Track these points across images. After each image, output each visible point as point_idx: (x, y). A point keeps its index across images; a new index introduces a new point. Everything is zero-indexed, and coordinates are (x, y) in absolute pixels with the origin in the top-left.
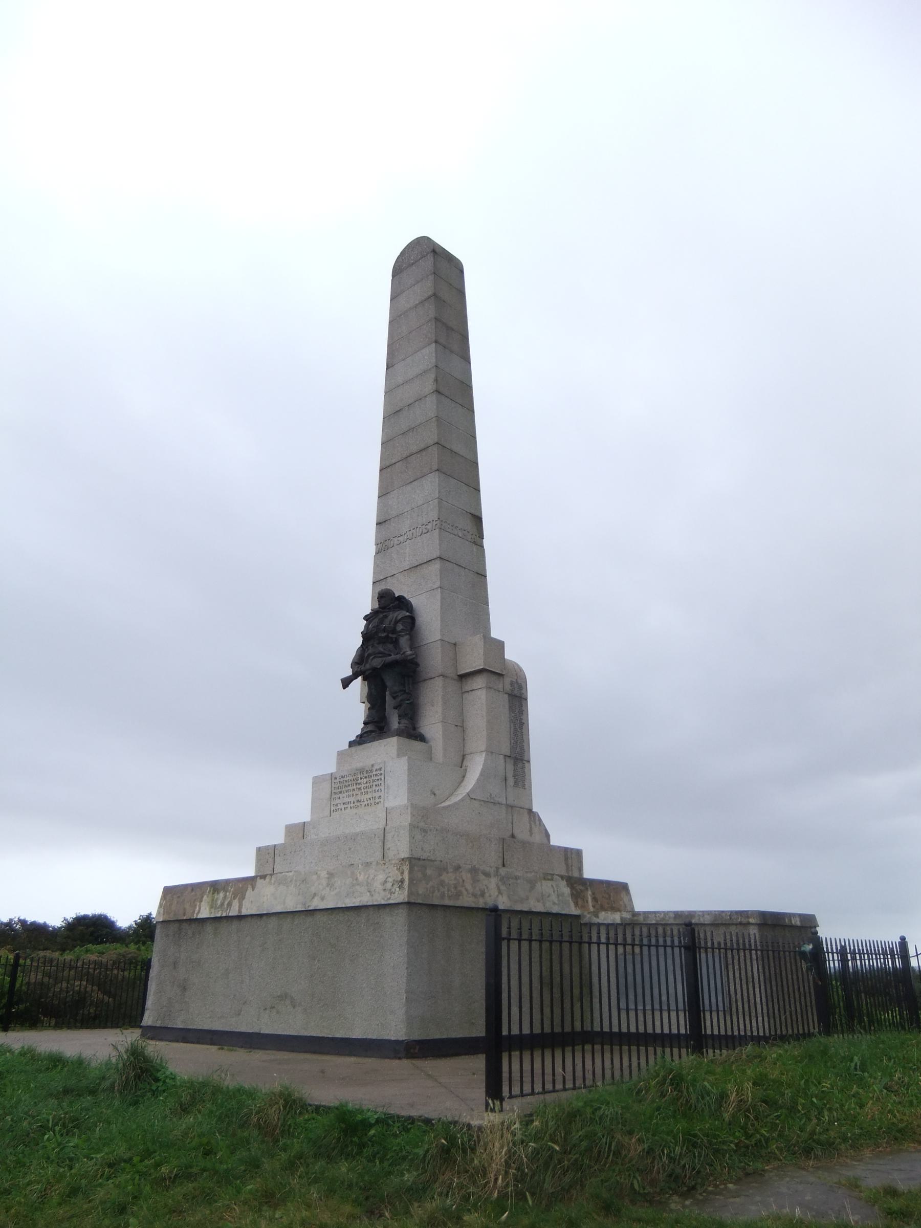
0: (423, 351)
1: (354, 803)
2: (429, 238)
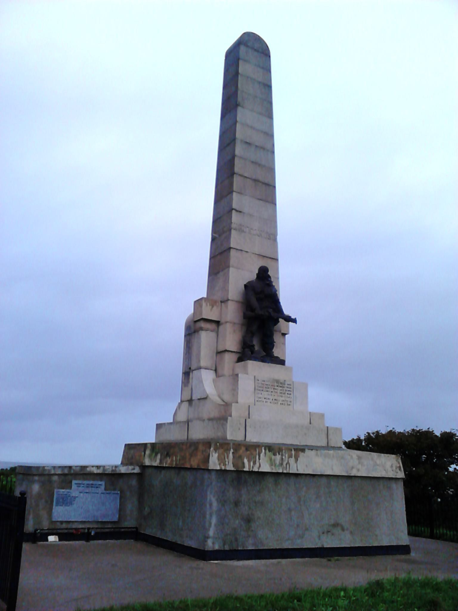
1: (272, 400)
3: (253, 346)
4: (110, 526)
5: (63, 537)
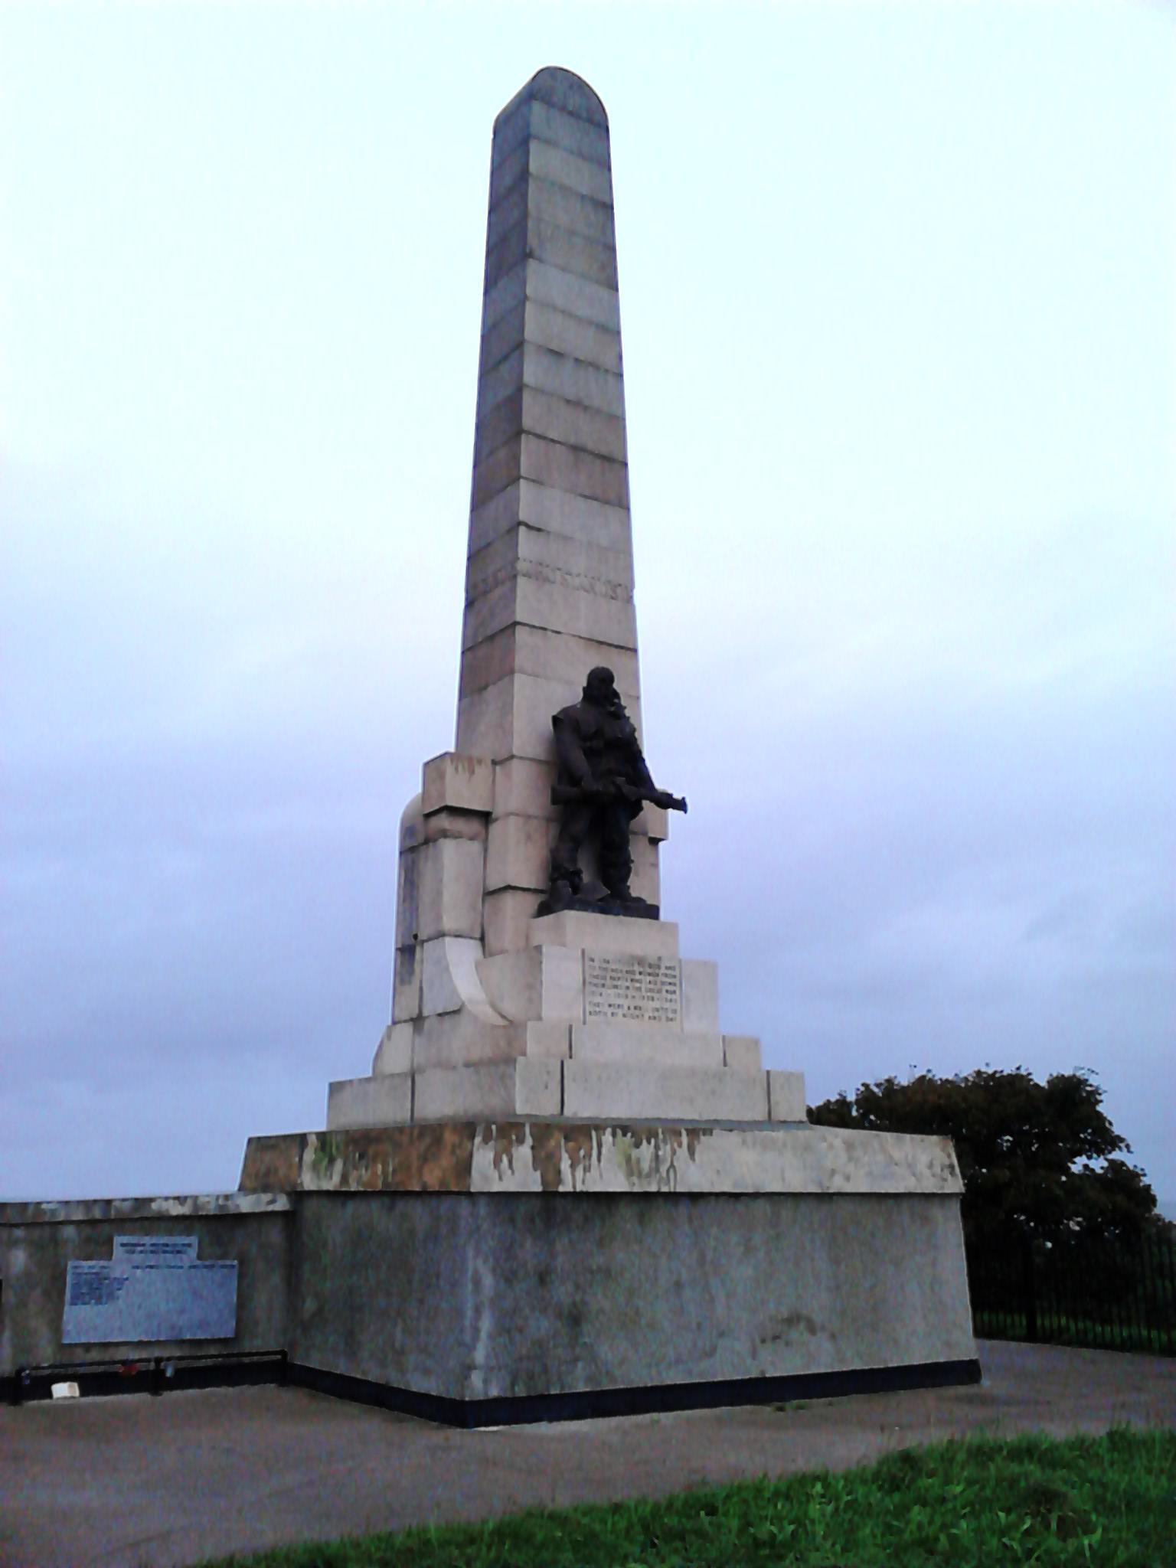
1: (629, 1008)
3: (578, 873)
4: (213, 1351)
5: (91, 1384)
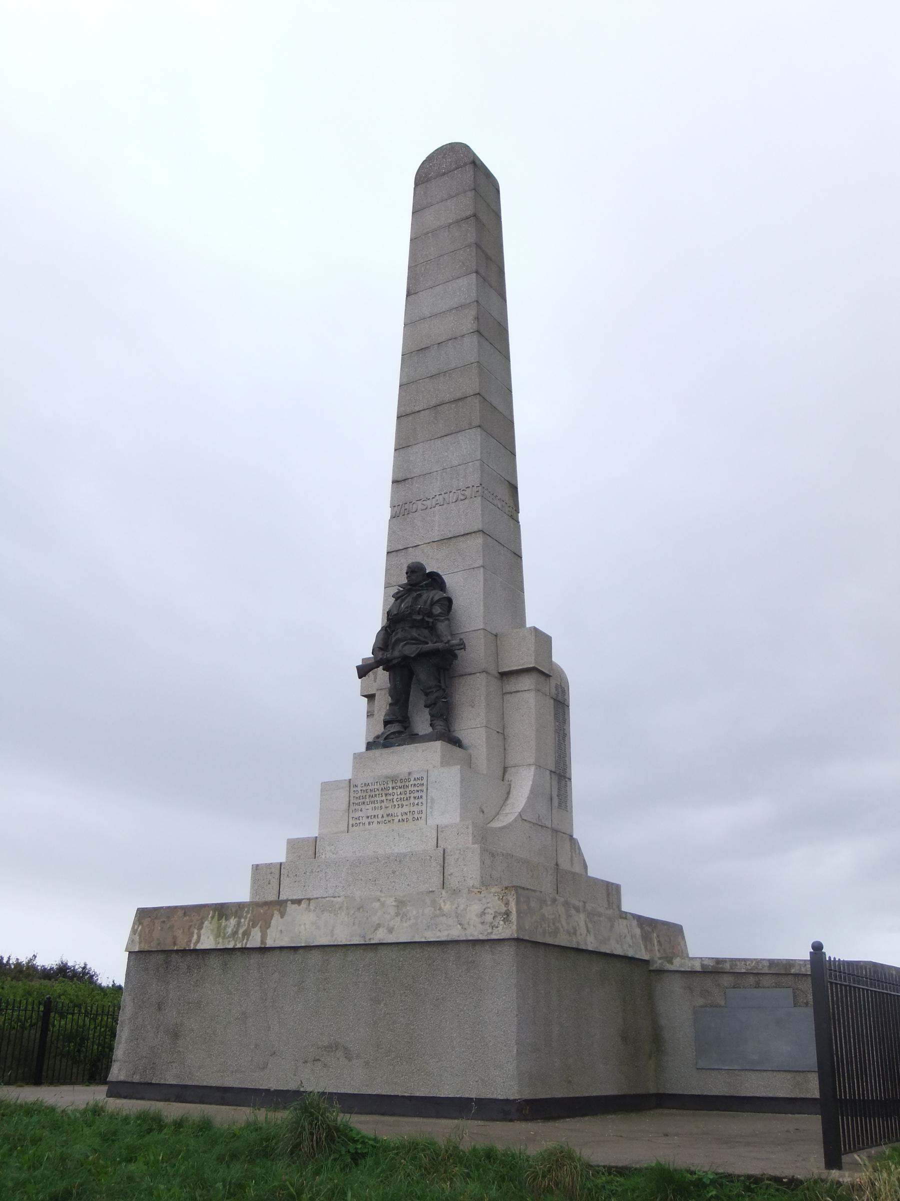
0: (460, 280)
1: (383, 817)
2: (468, 146)
